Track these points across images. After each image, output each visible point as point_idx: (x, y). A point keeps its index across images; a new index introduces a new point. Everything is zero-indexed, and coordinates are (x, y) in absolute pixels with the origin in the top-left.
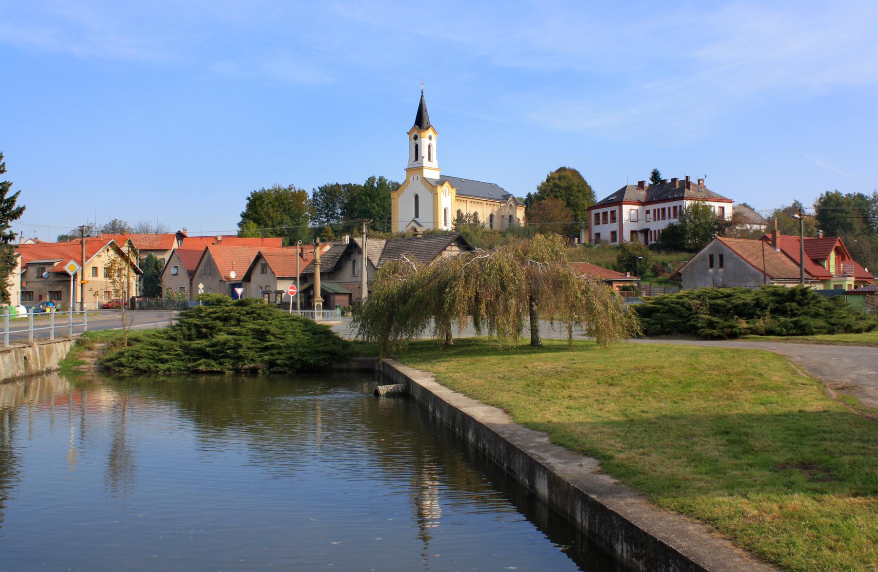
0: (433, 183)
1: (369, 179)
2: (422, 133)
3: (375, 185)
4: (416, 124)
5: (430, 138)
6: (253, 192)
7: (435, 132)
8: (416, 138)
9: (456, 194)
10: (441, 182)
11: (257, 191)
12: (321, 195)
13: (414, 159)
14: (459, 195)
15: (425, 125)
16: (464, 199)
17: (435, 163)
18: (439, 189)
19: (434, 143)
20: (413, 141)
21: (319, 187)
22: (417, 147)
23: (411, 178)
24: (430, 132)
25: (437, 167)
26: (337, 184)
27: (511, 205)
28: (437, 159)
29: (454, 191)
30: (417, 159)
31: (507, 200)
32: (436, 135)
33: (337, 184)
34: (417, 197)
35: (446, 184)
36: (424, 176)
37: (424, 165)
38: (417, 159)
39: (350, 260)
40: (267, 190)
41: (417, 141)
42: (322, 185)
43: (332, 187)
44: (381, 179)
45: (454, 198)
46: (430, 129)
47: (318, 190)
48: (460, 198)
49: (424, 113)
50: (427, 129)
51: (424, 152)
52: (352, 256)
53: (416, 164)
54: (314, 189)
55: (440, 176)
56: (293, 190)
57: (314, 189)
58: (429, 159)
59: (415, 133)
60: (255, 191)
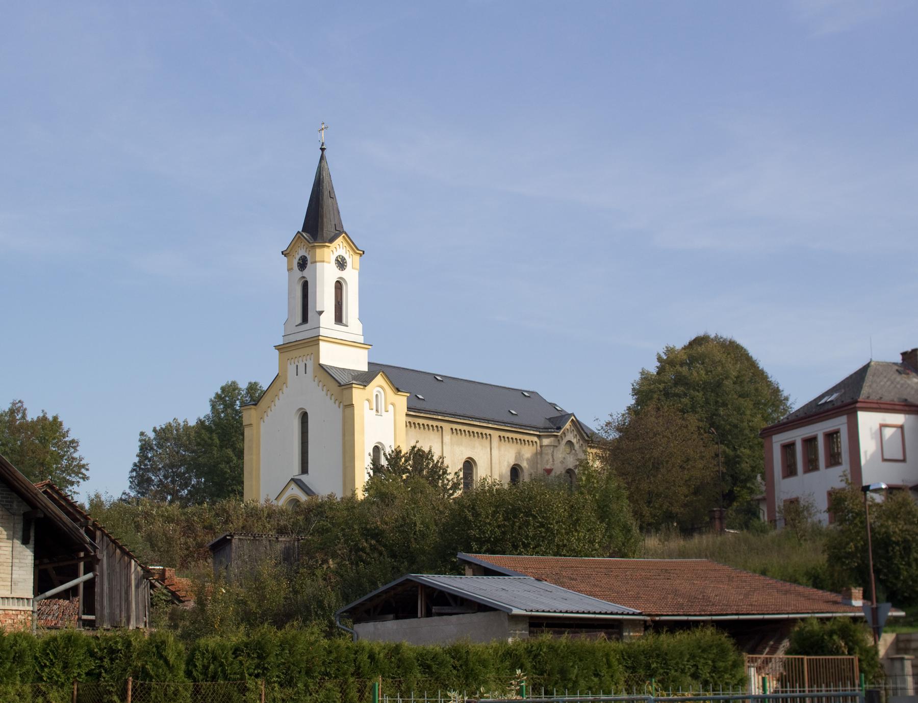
0: (343, 380)
1: (223, 389)
2: (318, 251)
4: (305, 228)
5: (341, 263)
7: (354, 247)
9: (409, 409)
10: (365, 379)
13: (299, 319)
14: (419, 411)
15: (328, 229)
16: (435, 423)
17: (354, 326)
18: (358, 394)
19: (351, 276)
20: (298, 274)
21: (155, 430)
23: (291, 369)
24: (339, 248)
25: (361, 339)
27: (570, 443)
28: (363, 317)
29: (402, 401)
30: (305, 319)
31: (559, 428)
32: (357, 258)
34: (304, 417)
35: (379, 380)
36: (322, 362)
37: (323, 332)
38: (305, 319)
41: (306, 273)
42: (160, 424)
45: (403, 419)
46: (340, 240)
47: (152, 435)
48: (421, 421)
49: (327, 201)
50: (331, 240)
51: (325, 300)
53: (304, 333)
54: (142, 434)
55: (369, 363)
57: (142, 434)
58: (339, 319)
59: (302, 252)
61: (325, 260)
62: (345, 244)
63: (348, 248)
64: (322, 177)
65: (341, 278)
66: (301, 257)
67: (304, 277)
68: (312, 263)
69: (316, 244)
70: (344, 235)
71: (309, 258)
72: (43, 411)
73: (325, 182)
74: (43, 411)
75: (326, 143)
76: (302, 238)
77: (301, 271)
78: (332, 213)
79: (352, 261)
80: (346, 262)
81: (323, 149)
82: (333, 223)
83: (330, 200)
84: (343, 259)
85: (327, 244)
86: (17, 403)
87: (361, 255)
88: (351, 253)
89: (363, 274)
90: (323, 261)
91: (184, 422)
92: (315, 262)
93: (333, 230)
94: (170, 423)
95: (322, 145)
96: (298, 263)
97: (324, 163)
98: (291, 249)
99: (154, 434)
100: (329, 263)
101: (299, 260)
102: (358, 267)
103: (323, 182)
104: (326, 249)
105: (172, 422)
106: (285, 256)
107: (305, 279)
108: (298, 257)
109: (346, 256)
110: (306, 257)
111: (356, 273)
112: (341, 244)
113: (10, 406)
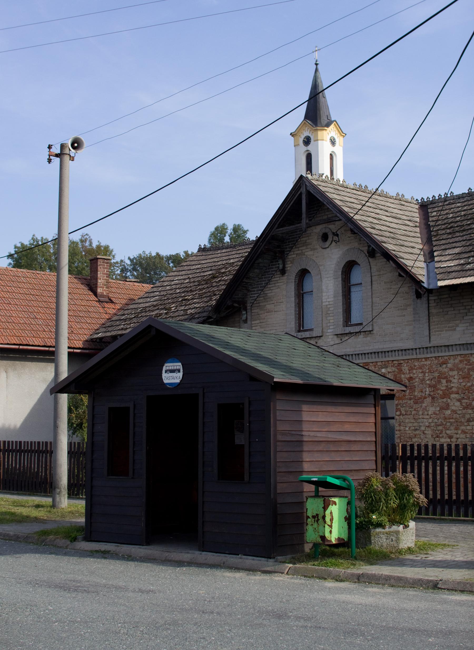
1: (217, 229)
2: (319, 133)
3: (227, 239)
5: (333, 142)
6: (19, 245)
8: (307, 141)
11: (27, 243)
12: (134, 269)
15: (324, 120)
19: (338, 150)
20: (303, 148)
21: (129, 258)
22: (309, 157)
24: (331, 132)
26: (158, 254)
32: (342, 138)
33: (158, 254)
39: (283, 272)
40: (39, 238)
41: (310, 148)
42: (134, 254)
43: (151, 258)
44: (237, 229)
46: (332, 126)
47: (128, 262)
50: (328, 125)
52: (292, 256)
56: (87, 244)
59: (306, 133)
60: (22, 244)
61: (324, 139)
62: (335, 129)
63: (337, 132)
64: (317, 83)
65: (333, 152)
66: (306, 137)
67: (308, 151)
68: (315, 141)
69: (318, 128)
70: (335, 122)
71: (312, 137)
72: (99, 241)
73: (320, 87)
74: (99, 241)
75: (318, 60)
76: (307, 123)
77: (306, 146)
78: (325, 107)
79: (339, 140)
80: (335, 141)
81: (316, 64)
82: (326, 115)
83: (323, 99)
84: (334, 139)
85: (326, 128)
86: (85, 236)
87: (344, 136)
88: (339, 135)
89: (345, 151)
90: (323, 140)
91: (149, 253)
92: (318, 140)
93: (326, 119)
94: (140, 254)
95: (316, 61)
96: (303, 141)
97: (318, 74)
98: (298, 132)
99: (129, 261)
100: (326, 141)
101: (304, 138)
102: (342, 145)
103: (318, 86)
104: (324, 132)
105: (142, 254)
106: (292, 136)
107: (309, 152)
108: (303, 137)
109: (336, 137)
110: (310, 137)
111: (341, 148)
112: (333, 129)
113: (80, 237)
